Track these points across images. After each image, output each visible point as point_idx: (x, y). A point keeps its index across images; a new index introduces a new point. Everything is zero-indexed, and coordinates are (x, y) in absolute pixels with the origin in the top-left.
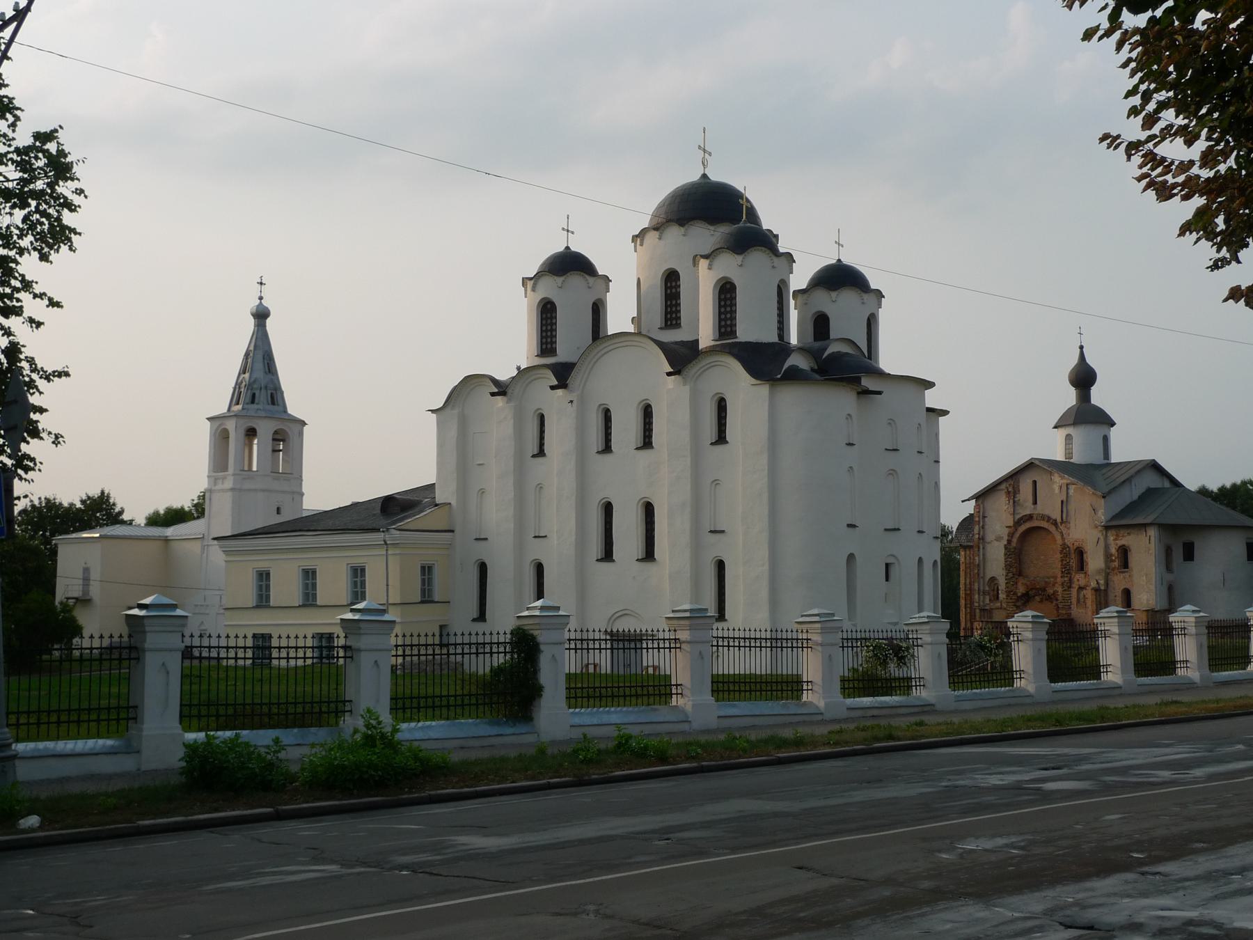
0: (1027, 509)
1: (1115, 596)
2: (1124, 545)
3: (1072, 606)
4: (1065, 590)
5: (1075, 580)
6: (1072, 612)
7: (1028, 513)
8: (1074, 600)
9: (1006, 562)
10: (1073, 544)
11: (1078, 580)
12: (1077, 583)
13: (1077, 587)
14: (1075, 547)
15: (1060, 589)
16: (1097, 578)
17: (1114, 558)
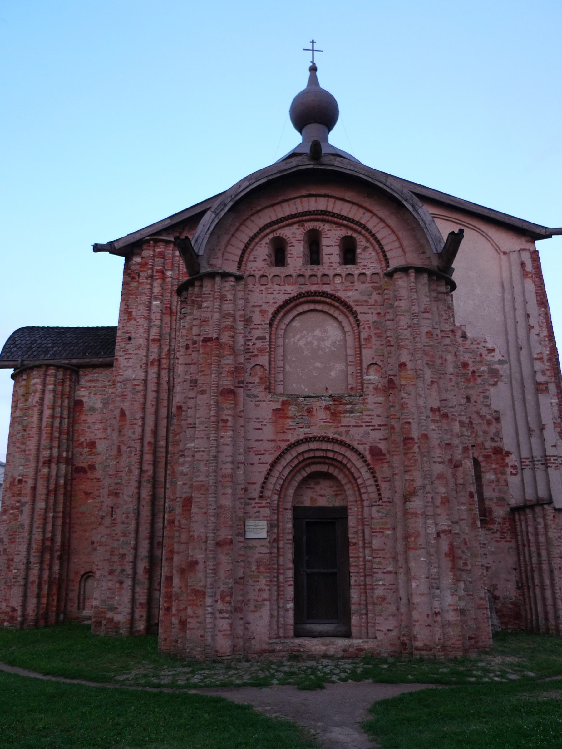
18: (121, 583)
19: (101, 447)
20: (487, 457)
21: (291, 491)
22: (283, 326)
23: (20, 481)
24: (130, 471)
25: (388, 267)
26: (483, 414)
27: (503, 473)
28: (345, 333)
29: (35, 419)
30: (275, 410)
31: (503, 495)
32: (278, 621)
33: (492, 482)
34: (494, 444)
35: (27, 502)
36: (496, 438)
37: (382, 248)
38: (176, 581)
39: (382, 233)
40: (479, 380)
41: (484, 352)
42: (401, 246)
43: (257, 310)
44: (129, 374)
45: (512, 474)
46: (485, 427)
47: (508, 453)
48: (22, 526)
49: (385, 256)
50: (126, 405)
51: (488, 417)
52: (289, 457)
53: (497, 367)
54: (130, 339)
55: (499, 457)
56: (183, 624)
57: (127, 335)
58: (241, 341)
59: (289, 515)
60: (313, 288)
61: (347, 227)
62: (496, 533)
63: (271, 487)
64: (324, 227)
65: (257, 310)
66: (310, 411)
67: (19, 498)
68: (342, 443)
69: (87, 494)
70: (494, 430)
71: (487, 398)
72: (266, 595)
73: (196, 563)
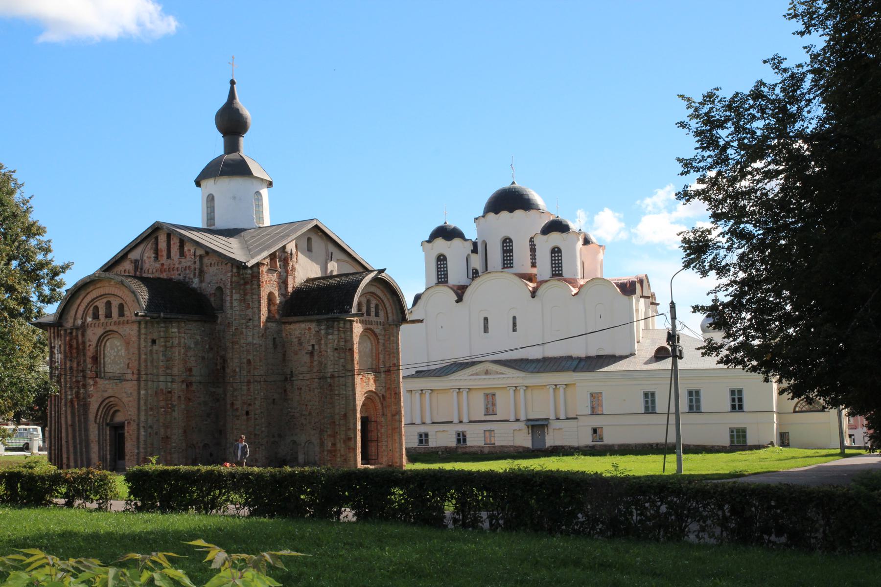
18: (259, 448)
19: (194, 369)
23: (170, 392)
24: (258, 393)
25: (388, 320)
28: (372, 346)
29: (177, 354)
35: (175, 405)
37: (386, 311)
38: (338, 445)
39: (388, 305)
42: (392, 312)
44: (250, 339)
48: (175, 419)
49: (387, 315)
50: (250, 357)
54: (250, 320)
56: (345, 459)
57: (248, 317)
60: (369, 326)
61: (378, 300)
64: (372, 299)
66: (369, 379)
67: (170, 402)
69: (189, 399)
73: (351, 438)
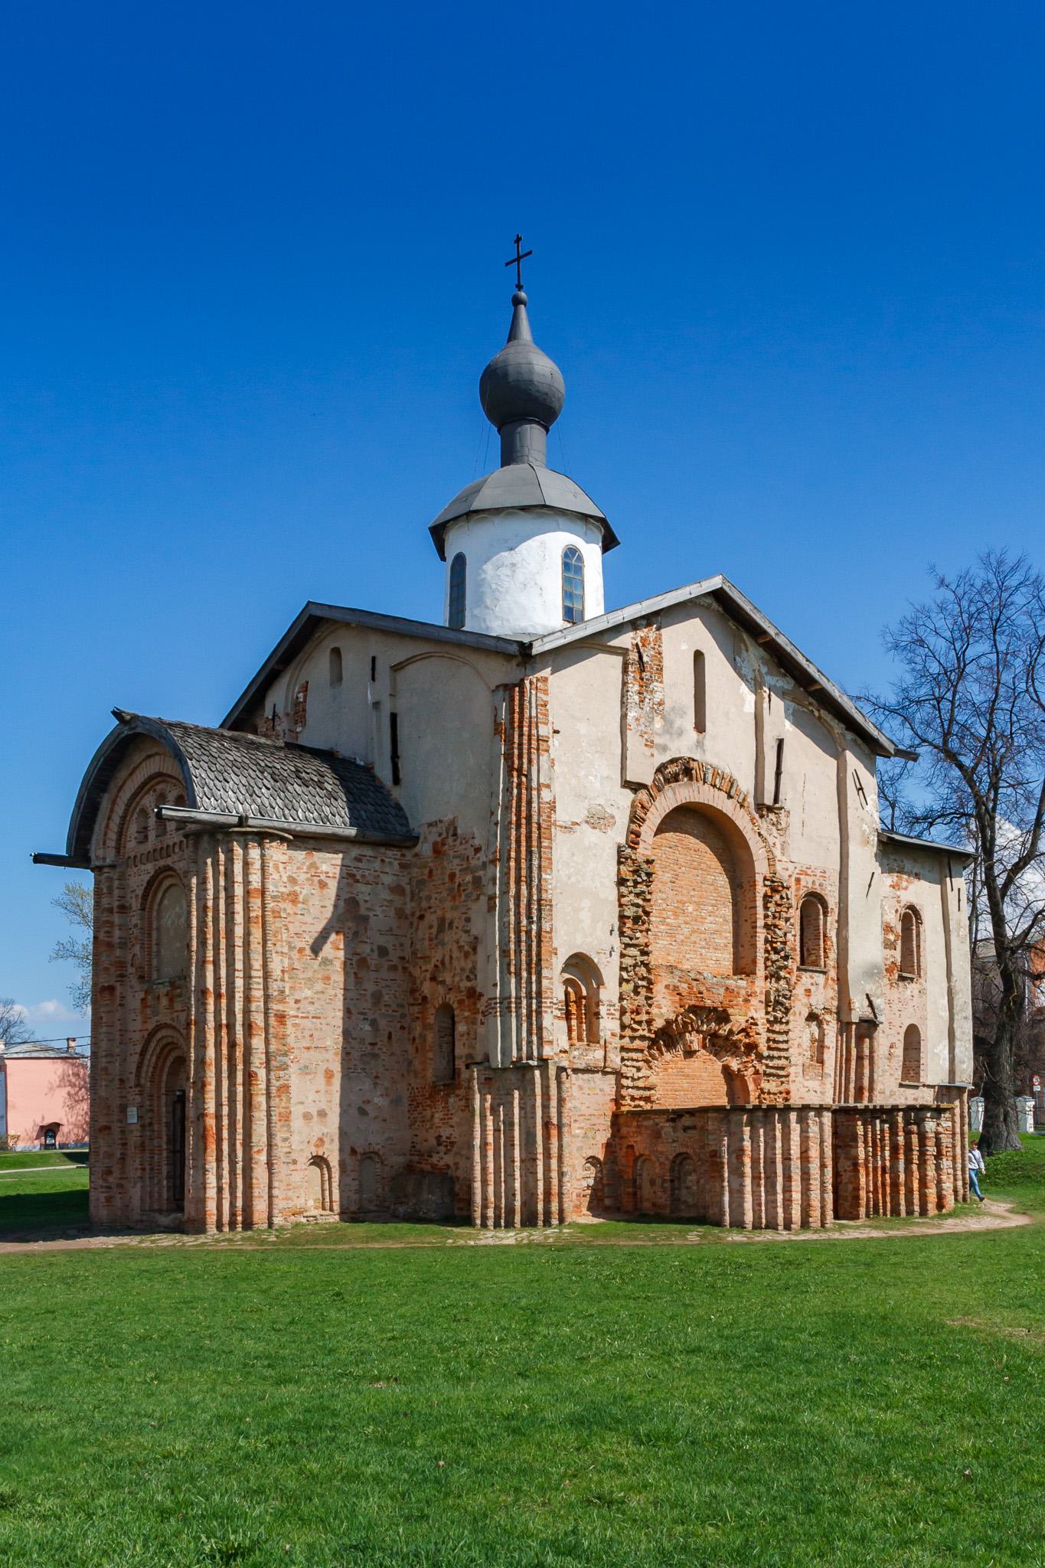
0: (684, 746)
1: (891, 1047)
2: (912, 907)
3: (792, 1070)
4: (777, 1021)
5: (799, 991)
6: (792, 1087)
7: (686, 754)
8: (793, 1052)
9: (621, 905)
10: (798, 880)
11: (808, 991)
12: (805, 1000)
13: (805, 1013)
14: (802, 892)
15: (760, 1015)
16: (870, 988)
17: (892, 937)
20: (461, 1002)
21: (164, 1077)
22: (156, 907)
26: (462, 944)
27: (474, 1023)
30: (143, 1000)
31: (471, 1051)
32: (151, 1196)
33: (462, 1036)
34: (469, 984)
36: (472, 977)
40: (463, 898)
41: (471, 852)
43: (133, 895)
45: (482, 1023)
46: (463, 964)
47: (481, 995)
51: (467, 948)
52: (153, 1045)
53: (481, 873)
55: (472, 1000)
58: (117, 933)
59: (163, 1099)
62: (461, 1100)
63: (143, 1074)
65: (133, 895)
66: (158, 998)
68: (174, 1028)
70: (470, 966)
71: (468, 920)
72: (139, 1173)
